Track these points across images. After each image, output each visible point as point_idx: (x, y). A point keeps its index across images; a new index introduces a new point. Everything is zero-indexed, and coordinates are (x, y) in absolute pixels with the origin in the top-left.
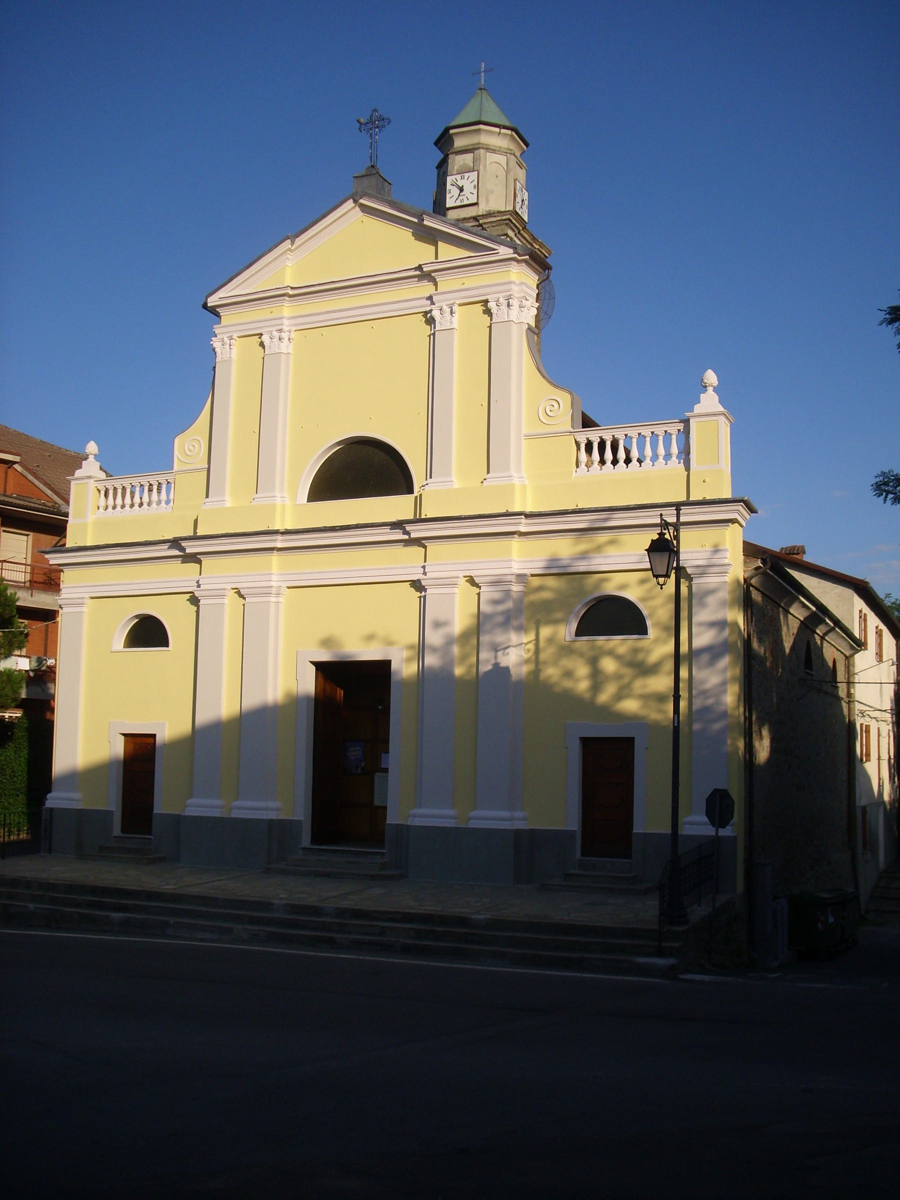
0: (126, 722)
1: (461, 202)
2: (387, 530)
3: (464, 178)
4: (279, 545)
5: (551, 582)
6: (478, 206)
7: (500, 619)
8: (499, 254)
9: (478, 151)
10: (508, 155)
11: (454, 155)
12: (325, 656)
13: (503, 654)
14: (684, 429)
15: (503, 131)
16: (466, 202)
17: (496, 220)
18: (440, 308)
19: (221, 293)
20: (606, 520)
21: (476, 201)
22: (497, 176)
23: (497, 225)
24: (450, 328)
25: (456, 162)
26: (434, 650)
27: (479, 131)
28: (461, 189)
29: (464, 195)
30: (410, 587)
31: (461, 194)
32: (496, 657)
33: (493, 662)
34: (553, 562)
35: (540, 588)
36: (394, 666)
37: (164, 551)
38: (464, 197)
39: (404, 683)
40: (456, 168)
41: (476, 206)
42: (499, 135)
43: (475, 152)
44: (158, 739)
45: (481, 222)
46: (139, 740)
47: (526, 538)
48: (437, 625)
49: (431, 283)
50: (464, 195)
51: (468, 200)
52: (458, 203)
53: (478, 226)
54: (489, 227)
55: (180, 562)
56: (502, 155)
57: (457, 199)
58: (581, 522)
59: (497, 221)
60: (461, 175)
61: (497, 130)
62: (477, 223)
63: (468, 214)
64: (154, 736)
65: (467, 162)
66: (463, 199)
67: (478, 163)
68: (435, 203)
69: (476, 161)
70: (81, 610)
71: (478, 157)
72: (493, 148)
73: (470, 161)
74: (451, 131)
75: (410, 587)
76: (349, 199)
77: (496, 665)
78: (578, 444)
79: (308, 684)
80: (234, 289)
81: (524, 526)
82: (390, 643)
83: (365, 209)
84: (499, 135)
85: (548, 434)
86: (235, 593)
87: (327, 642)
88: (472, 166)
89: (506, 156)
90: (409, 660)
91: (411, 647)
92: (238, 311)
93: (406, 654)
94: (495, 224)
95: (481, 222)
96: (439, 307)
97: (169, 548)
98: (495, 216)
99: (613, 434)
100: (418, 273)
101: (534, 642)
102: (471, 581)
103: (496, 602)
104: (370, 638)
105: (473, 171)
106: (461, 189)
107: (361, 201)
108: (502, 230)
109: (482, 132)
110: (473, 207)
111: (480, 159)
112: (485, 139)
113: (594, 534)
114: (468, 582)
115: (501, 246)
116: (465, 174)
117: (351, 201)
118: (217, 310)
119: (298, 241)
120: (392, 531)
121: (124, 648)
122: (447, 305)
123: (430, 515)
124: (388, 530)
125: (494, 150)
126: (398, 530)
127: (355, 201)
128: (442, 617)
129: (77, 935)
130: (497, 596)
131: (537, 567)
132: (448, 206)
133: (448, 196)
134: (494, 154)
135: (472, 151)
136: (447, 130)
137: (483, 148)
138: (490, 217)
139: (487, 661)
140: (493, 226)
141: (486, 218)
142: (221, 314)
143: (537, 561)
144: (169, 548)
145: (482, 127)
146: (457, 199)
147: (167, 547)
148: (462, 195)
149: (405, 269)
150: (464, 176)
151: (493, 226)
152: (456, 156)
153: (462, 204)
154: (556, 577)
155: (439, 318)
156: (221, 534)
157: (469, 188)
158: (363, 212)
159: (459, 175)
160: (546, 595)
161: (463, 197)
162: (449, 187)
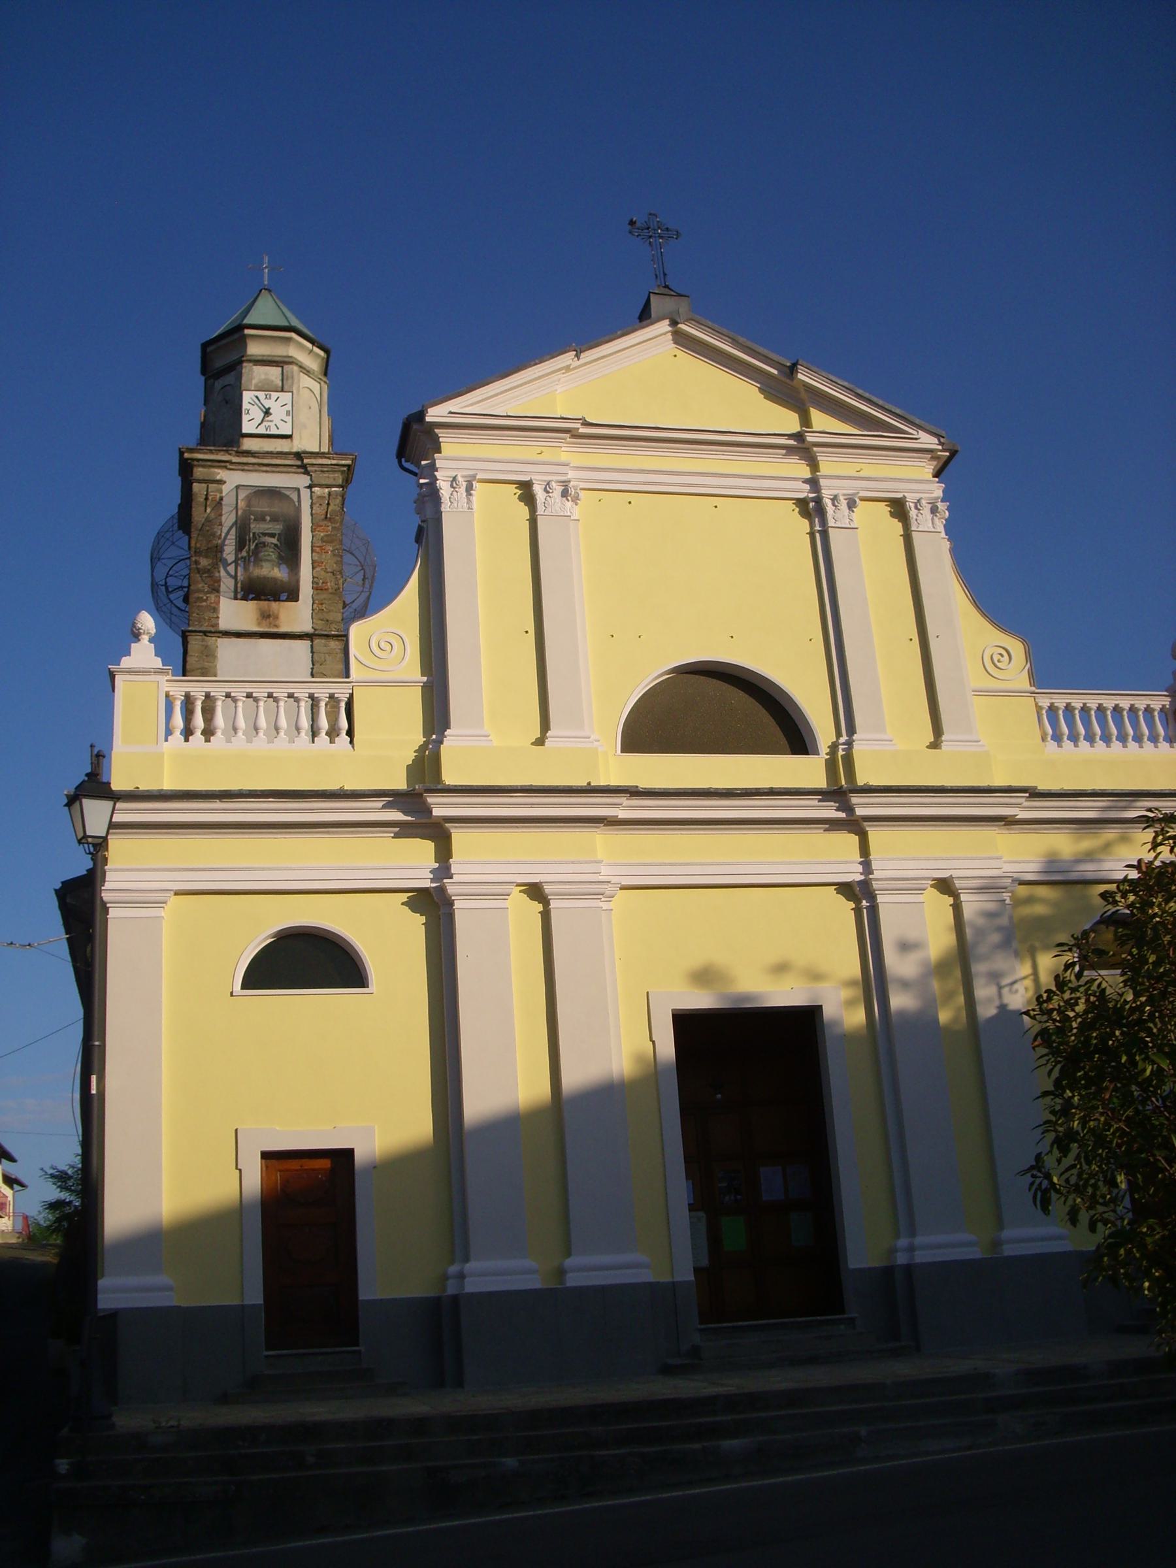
0: (278, 1128)
1: (267, 430)
2: (813, 801)
3: (270, 398)
4: (622, 814)
5: (1043, 892)
6: (292, 440)
7: (996, 938)
8: (918, 441)
9: (291, 366)
10: (322, 383)
11: (251, 364)
12: (701, 1000)
13: (1010, 990)
14: (1170, 705)
15: (316, 350)
16: (274, 431)
17: (329, 463)
18: (832, 497)
19: (455, 405)
20: (1125, 808)
21: (290, 433)
22: (310, 408)
23: (327, 471)
24: (849, 526)
25: (255, 374)
26: (905, 984)
27: (289, 339)
28: (267, 412)
29: (271, 421)
30: (837, 893)
31: (267, 419)
32: (1000, 995)
33: (997, 1003)
34: (1052, 863)
35: (1030, 900)
36: (829, 1012)
37: (374, 812)
38: (272, 424)
39: (847, 1038)
40: (254, 382)
41: (289, 440)
42: (309, 354)
43: (286, 367)
44: (359, 1157)
45: (306, 461)
46: (294, 1165)
47: (1008, 829)
48: (905, 947)
49: (803, 462)
50: (271, 421)
51: (278, 428)
52: (261, 430)
53: (298, 467)
54: (316, 471)
55: (392, 835)
56: (315, 380)
57: (259, 425)
58: (1088, 810)
59: (332, 465)
60: (266, 393)
61: (309, 345)
62: (299, 463)
63: (276, 448)
64: (350, 1152)
65: (273, 378)
66: (269, 426)
67: (290, 381)
68: (203, 425)
69: (287, 379)
70: (158, 915)
71: (290, 375)
72: (308, 369)
73: (276, 378)
74: (247, 332)
75: (837, 893)
76: (667, 319)
77: (1003, 1008)
78: (1039, 709)
79: (667, 1048)
80: (466, 406)
81: (1023, 810)
82: (816, 976)
83: (682, 340)
84: (309, 354)
85: (981, 692)
86: (520, 891)
87: (704, 976)
88: (280, 384)
89: (320, 383)
90: (850, 1003)
91: (851, 983)
92: (474, 441)
93: (845, 994)
94: (326, 469)
95: (306, 461)
96: (831, 495)
97: (384, 807)
98: (329, 458)
99: (1084, 701)
100: (792, 442)
101: (1032, 977)
102: (945, 886)
103: (990, 915)
104: (781, 969)
105: (282, 390)
106: (267, 412)
107: (682, 326)
108: (334, 479)
109: (291, 344)
110: (284, 440)
111: (292, 377)
112: (293, 352)
113: (1100, 829)
114: (935, 888)
115: (920, 431)
116: (272, 393)
117: (667, 322)
118: (437, 431)
119: (587, 356)
120: (821, 804)
121: (242, 988)
122: (844, 495)
123: (875, 782)
124: (816, 803)
125: (308, 371)
126: (832, 804)
127: (674, 323)
128: (912, 935)
129: (643, 1498)
130: (991, 906)
131: (1030, 868)
132: (244, 431)
133: (245, 418)
134: (306, 376)
135: (281, 365)
136: (239, 328)
137: (297, 364)
138: (321, 458)
139: (989, 1000)
140: (322, 471)
141: (315, 458)
142: (441, 440)
143: (1029, 862)
144: (384, 807)
145: (293, 335)
146: (259, 425)
147: (380, 805)
148: (268, 421)
149: (777, 432)
150: (270, 395)
151: (322, 471)
152: (254, 367)
153: (268, 432)
154: (1062, 886)
155: (832, 512)
156: (521, 786)
157: (278, 413)
158: (675, 343)
159: (263, 393)
160: (1039, 909)
161: (269, 423)
162: (245, 405)
